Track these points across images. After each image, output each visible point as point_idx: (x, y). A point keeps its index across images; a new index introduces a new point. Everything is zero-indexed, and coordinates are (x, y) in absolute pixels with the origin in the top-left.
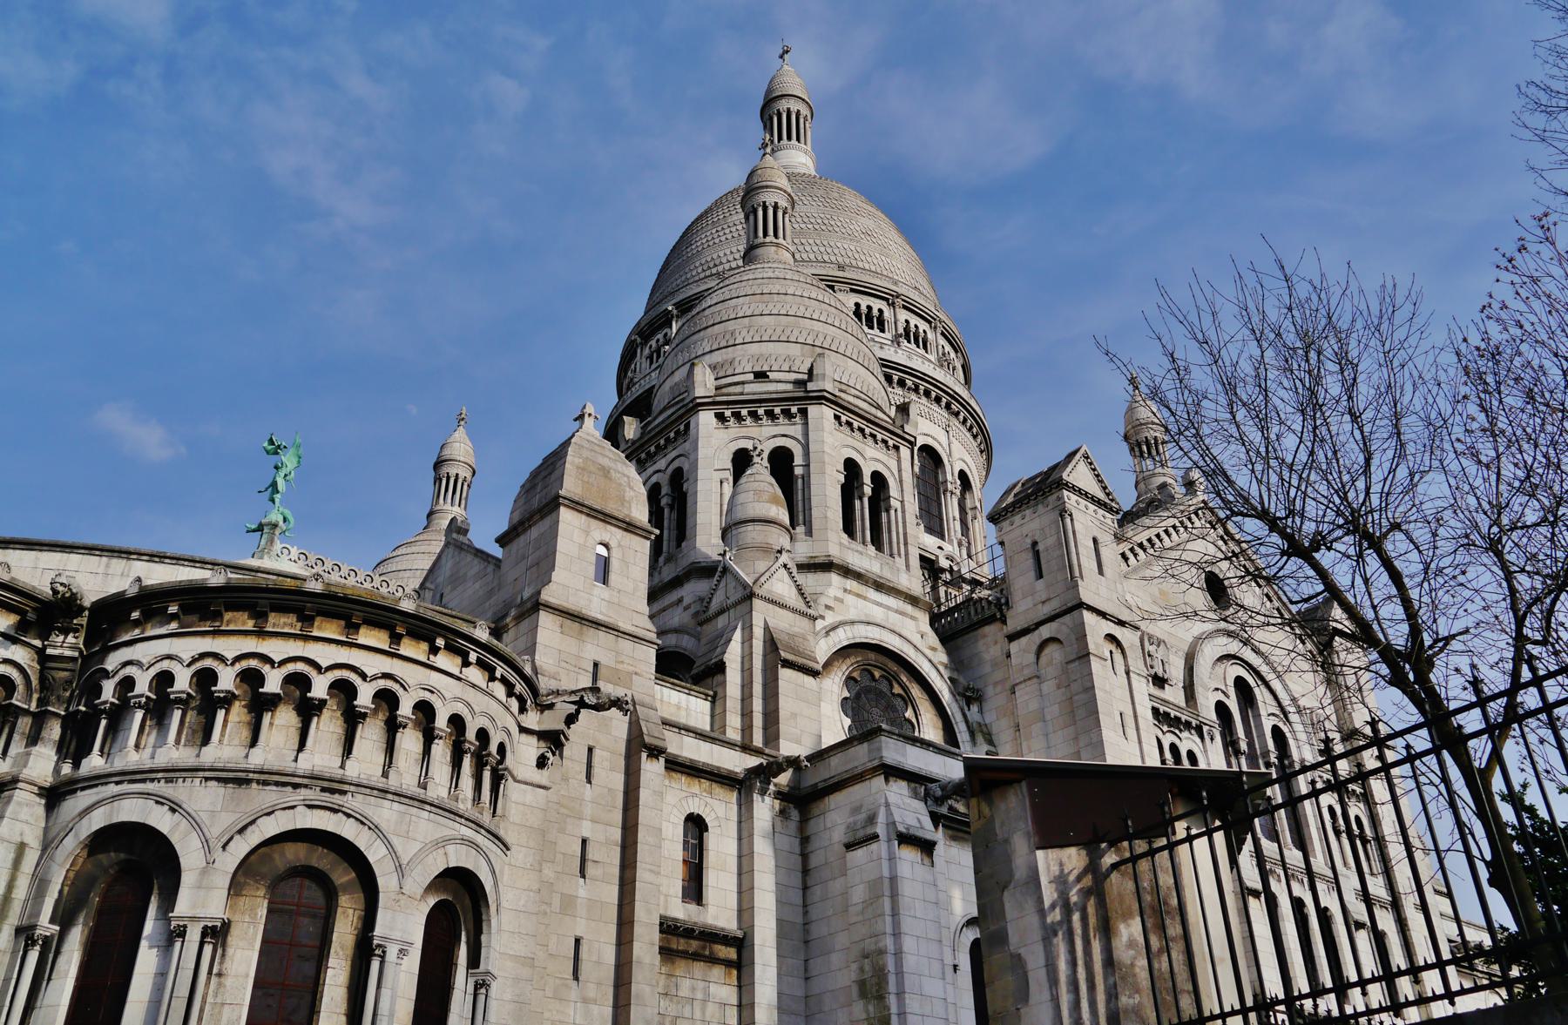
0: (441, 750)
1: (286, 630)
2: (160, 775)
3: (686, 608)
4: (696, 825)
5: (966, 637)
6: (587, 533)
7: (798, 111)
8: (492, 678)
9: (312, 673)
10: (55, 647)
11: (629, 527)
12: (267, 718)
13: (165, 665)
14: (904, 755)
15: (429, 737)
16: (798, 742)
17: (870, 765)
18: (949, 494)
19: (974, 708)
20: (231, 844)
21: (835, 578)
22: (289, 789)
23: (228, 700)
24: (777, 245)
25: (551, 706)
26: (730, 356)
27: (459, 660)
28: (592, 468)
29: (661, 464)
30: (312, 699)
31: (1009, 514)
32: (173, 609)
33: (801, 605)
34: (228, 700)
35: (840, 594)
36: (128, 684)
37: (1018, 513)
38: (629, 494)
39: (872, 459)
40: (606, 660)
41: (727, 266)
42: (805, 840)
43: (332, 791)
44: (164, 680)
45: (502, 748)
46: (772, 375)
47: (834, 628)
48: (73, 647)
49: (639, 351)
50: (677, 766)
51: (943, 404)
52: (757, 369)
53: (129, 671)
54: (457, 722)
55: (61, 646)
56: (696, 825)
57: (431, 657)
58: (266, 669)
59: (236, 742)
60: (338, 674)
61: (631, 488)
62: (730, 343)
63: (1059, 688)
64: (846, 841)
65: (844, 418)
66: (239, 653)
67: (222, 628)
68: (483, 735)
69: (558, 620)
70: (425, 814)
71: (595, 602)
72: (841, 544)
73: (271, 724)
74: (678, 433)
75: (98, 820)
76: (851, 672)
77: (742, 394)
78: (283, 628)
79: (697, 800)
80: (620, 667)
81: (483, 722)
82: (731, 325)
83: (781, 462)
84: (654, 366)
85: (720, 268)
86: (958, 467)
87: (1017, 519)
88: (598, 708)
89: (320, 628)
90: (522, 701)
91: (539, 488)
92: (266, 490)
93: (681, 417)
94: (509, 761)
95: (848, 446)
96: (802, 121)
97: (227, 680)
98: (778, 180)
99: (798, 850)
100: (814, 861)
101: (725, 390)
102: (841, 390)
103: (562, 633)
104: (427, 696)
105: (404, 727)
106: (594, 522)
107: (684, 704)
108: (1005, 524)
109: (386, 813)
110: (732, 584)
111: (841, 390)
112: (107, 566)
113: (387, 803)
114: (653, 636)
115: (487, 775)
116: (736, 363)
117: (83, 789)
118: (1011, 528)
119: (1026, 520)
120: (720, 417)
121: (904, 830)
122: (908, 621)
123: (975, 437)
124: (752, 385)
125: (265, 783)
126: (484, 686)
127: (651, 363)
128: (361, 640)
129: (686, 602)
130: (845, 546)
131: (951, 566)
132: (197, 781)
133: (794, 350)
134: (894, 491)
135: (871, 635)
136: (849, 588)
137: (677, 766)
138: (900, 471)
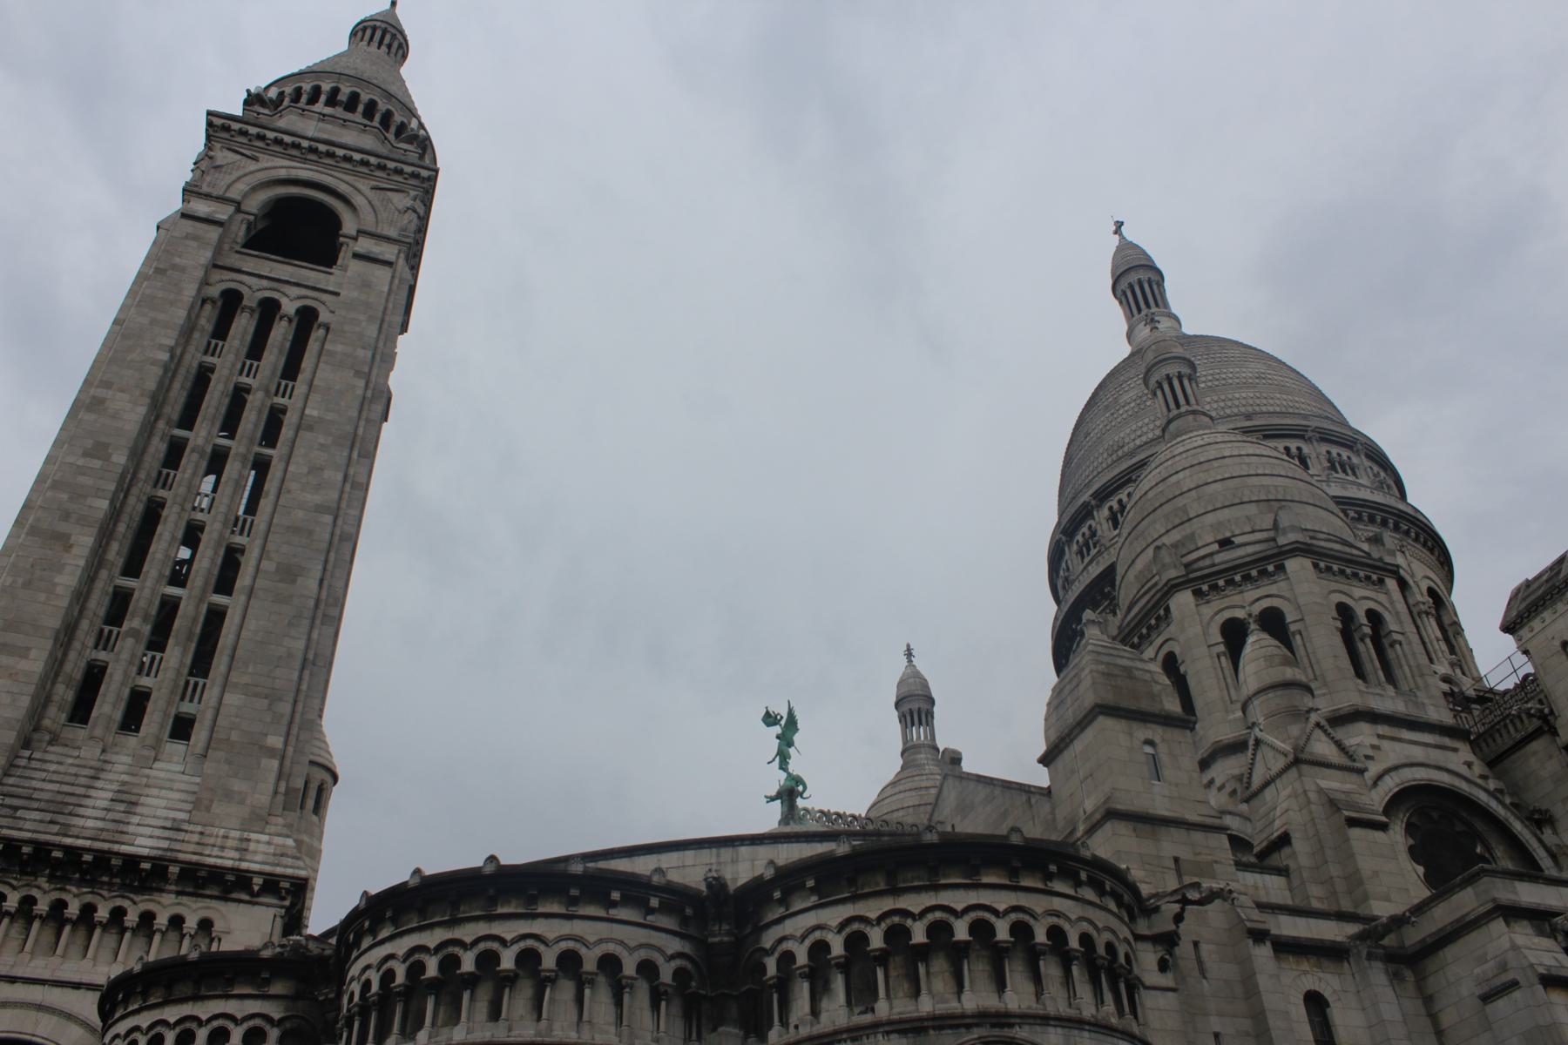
1: (916, 884)
2: (844, 1036)
3: (1220, 789)
4: (1315, 1002)
5: (1514, 757)
6: (1131, 735)
7: (1149, 279)
8: (1101, 892)
9: (952, 919)
10: (715, 936)
12: (922, 970)
13: (817, 935)
14: (1516, 893)
15: (1066, 959)
16: (1388, 899)
17: (1482, 910)
18: (1424, 616)
19: (1548, 832)
21: (1364, 727)
22: (963, 1030)
24: (1194, 412)
25: (1156, 909)
26: (1189, 531)
28: (1116, 672)
30: (959, 942)
31: (1525, 620)
32: (810, 883)
33: (1344, 761)
34: (882, 958)
35: (1376, 741)
36: (788, 957)
37: (1535, 617)
38: (1157, 688)
39: (1361, 598)
40: (1185, 854)
41: (1132, 445)
42: (1428, 1000)
43: (1002, 1026)
44: (820, 949)
46: (1237, 540)
47: (1380, 777)
48: (729, 933)
49: (1066, 549)
50: (1287, 948)
51: (1391, 525)
52: (1220, 537)
54: (1085, 939)
55: (720, 934)
56: (1315, 1002)
57: (1049, 884)
58: (909, 922)
59: (901, 994)
60: (973, 915)
61: (1157, 682)
62: (1185, 518)
64: (1479, 992)
65: (1322, 565)
66: (881, 912)
67: (859, 892)
68: (1110, 947)
70: (1086, 1034)
72: (1360, 691)
73: (928, 973)
74: (1158, 619)
76: (1408, 819)
77: (1214, 565)
78: (912, 882)
79: (1309, 976)
80: (1199, 858)
81: (1107, 936)
82: (1180, 502)
83: (1273, 622)
84: (1087, 560)
85: (1126, 449)
86: (1424, 585)
87: (1536, 624)
88: (1200, 902)
89: (946, 876)
91: (1069, 701)
92: (774, 760)
93: (1157, 603)
95: (1334, 591)
96: (1155, 287)
97: (876, 939)
98: (1174, 350)
99: (1423, 1011)
100: (1447, 1020)
101: (1195, 566)
102: (1311, 538)
103: (1137, 837)
104: (1054, 920)
105: (1044, 954)
106: (1135, 725)
107: (1260, 884)
108: (1524, 633)
110: (1270, 754)
111: (1311, 538)
112: (718, 856)
113: (1051, 1030)
115: (1122, 986)
118: (1532, 634)
119: (1546, 623)
120: (1198, 593)
121: (1545, 972)
122: (1450, 754)
123: (1431, 551)
124: (1221, 555)
125: (941, 1028)
126: (1098, 901)
127: (1083, 558)
128: (985, 880)
129: (1218, 783)
130: (1364, 692)
131: (1451, 689)
132: (880, 1037)
133: (1252, 509)
134: (1392, 625)
135: (1418, 776)
136: (1381, 733)
137: (1287, 948)
138: (1392, 603)
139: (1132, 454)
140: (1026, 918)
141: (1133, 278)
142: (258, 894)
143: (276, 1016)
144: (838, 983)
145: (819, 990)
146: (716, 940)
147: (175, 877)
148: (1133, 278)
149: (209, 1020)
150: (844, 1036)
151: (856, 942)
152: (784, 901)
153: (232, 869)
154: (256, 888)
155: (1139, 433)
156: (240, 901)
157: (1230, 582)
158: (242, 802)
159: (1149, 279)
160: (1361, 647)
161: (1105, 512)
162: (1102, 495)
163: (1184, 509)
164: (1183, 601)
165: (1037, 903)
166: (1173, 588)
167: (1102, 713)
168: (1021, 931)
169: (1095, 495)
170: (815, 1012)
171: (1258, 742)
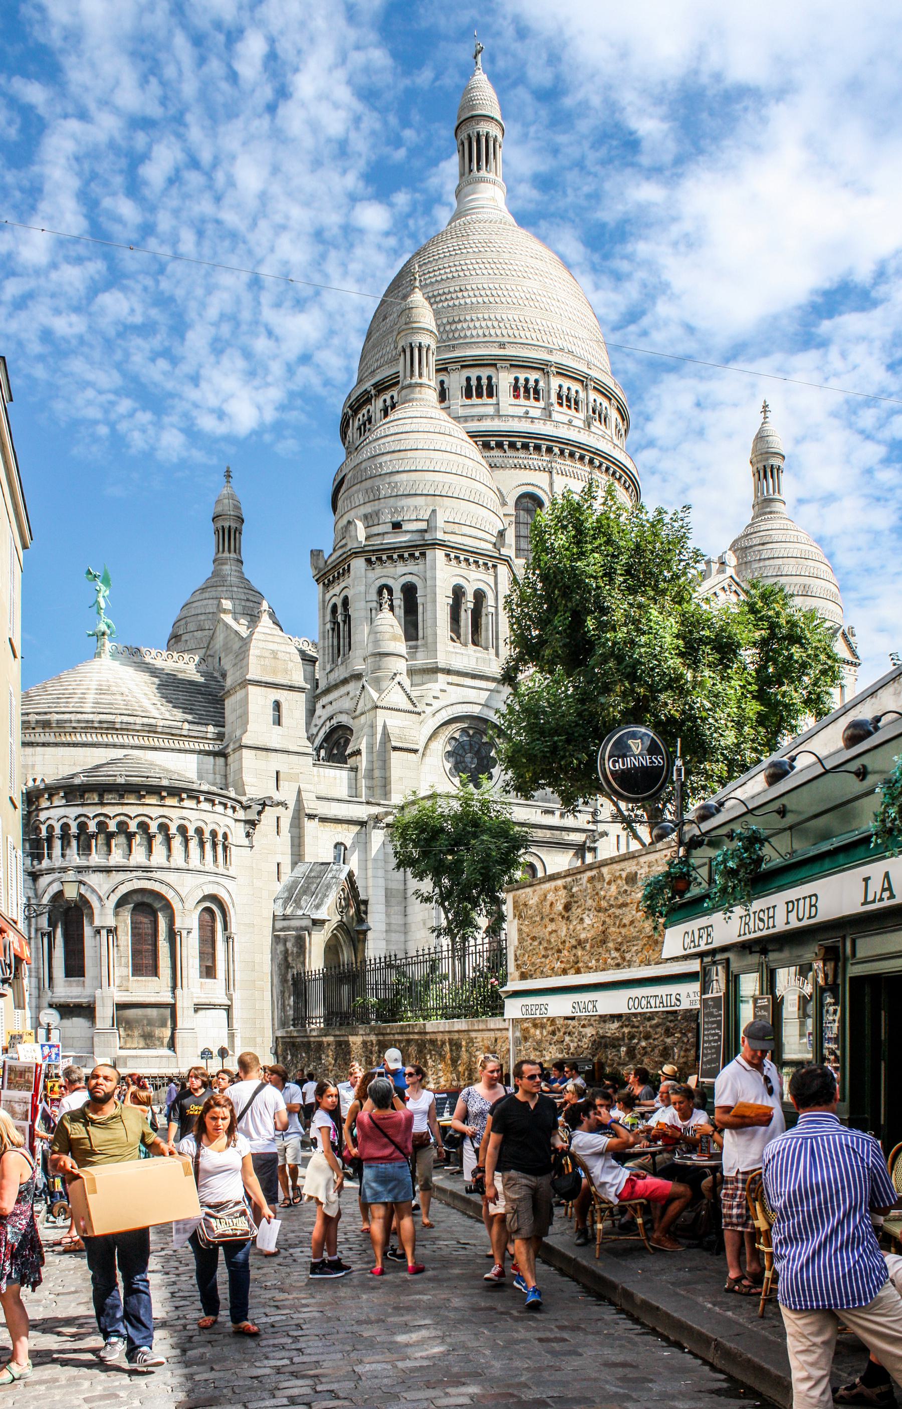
0: (193, 844)
11: (291, 688)
21: (440, 676)
23: (94, 836)
25: (250, 807)
26: (376, 508)
27: (195, 802)
28: (267, 654)
29: (337, 589)
33: (410, 707)
34: (94, 836)
35: (446, 687)
36: (51, 828)
45: (225, 836)
52: (394, 520)
53: (49, 822)
58: (107, 821)
65: (452, 555)
68: (214, 834)
69: (253, 752)
71: (274, 737)
81: (212, 826)
84: (362, 438)
90: (234, 809)
94: (230, 840)
97: (92, 827)
104: (182, 822)
109: (170, 877)
114: (310, 751)
120: (369, 561)
140: (167, 821)
144: (74, 843)
145: (66, 844)
151: (82, 826)
152: (50, 799)
157: (390, 558)
160: (463, 613)
164: (358, 564)
165: (174, 814)
166: (356, 554)
168: (163, 828)
169: (375, 385)
170: (63, 856)
171: (363, 687)
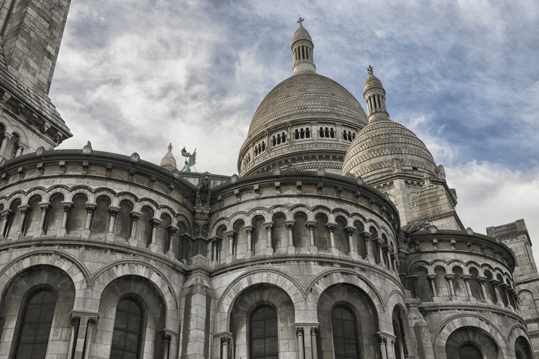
1: (490, 256)
13: (456, 263)
20: (510, 339)
32: (453, 241)
36: (440, 269)
46: (419, 169)
52: (413, 165)
53: (438, 263)
63: (530, 309)
75: (457, 324)
82: (398, 146)
84: (277, 145)
91: (430, 205)
96: (311, 52)
116: (404, 162)
117: (441, 310)
120: (406, 182)
133: (424, 161)
139: (314, 113)
141: (305, 44)
142: (44, 133)
143: (177, 212)
146: (404, 251)
147: (6, 100)
148: (305, 44)
149: (142, 200)
150: (476, 309)
153: (38, 112)
154: (46, 129)
155: (315, 107)
156: (35, 132)
158: (34, 75)
159: (307, 46)
161: (294, 131)
162: (295, 123)
163: (400, 148)
167: (454, 215)
169: (292, 122)
